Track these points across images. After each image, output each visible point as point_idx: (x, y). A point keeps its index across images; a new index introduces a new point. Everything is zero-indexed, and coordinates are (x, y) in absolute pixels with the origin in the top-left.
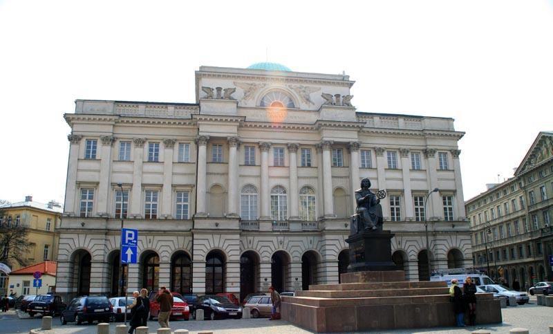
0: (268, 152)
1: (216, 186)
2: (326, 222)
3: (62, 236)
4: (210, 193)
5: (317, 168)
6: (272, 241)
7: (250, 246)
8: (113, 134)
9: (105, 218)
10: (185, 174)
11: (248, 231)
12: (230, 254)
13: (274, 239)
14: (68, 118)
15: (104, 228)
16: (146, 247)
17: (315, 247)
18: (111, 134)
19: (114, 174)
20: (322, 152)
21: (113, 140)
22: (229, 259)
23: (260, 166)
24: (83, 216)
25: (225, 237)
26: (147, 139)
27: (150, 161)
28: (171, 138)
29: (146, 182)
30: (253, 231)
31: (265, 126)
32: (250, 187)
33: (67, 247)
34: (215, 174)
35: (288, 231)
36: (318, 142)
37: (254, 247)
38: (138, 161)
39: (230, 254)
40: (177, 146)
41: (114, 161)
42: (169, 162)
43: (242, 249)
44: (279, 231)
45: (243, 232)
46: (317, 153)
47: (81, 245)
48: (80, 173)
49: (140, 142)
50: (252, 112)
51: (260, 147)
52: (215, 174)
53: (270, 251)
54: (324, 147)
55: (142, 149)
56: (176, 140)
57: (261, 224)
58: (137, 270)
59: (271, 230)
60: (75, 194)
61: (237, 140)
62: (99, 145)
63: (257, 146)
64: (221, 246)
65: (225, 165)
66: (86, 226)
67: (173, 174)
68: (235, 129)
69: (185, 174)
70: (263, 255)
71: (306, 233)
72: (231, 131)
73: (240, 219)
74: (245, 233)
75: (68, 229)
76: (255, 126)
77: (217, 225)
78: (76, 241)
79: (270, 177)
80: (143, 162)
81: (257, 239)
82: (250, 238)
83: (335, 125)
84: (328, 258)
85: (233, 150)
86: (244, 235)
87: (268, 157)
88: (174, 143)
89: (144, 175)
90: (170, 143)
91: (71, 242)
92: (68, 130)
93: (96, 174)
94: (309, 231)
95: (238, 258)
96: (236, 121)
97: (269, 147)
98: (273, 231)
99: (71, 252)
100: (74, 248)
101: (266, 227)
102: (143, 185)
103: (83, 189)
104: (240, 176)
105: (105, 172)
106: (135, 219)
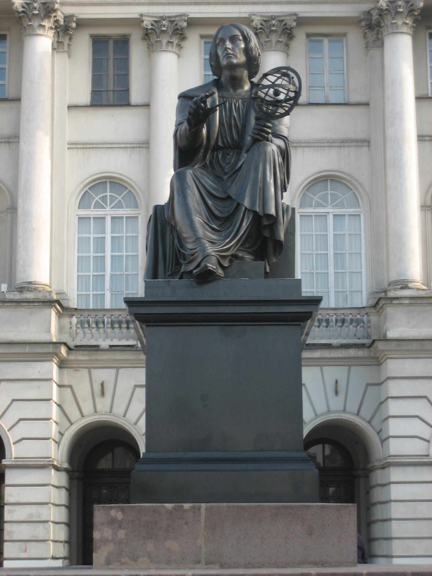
2: (389, 310)
5: (367, 104)
7: (103, 404)
11: (96, 348)
17: (352, 407)
20: (382, 46)
36: (366, 7)
37: (119, 409)
43: (74, 413)
46: (367, 47)
51: (147, 35)
54: (388, 20)
65: (13, 105)
84: (396, 447)
94: (329, 346)
95: (58, 453)
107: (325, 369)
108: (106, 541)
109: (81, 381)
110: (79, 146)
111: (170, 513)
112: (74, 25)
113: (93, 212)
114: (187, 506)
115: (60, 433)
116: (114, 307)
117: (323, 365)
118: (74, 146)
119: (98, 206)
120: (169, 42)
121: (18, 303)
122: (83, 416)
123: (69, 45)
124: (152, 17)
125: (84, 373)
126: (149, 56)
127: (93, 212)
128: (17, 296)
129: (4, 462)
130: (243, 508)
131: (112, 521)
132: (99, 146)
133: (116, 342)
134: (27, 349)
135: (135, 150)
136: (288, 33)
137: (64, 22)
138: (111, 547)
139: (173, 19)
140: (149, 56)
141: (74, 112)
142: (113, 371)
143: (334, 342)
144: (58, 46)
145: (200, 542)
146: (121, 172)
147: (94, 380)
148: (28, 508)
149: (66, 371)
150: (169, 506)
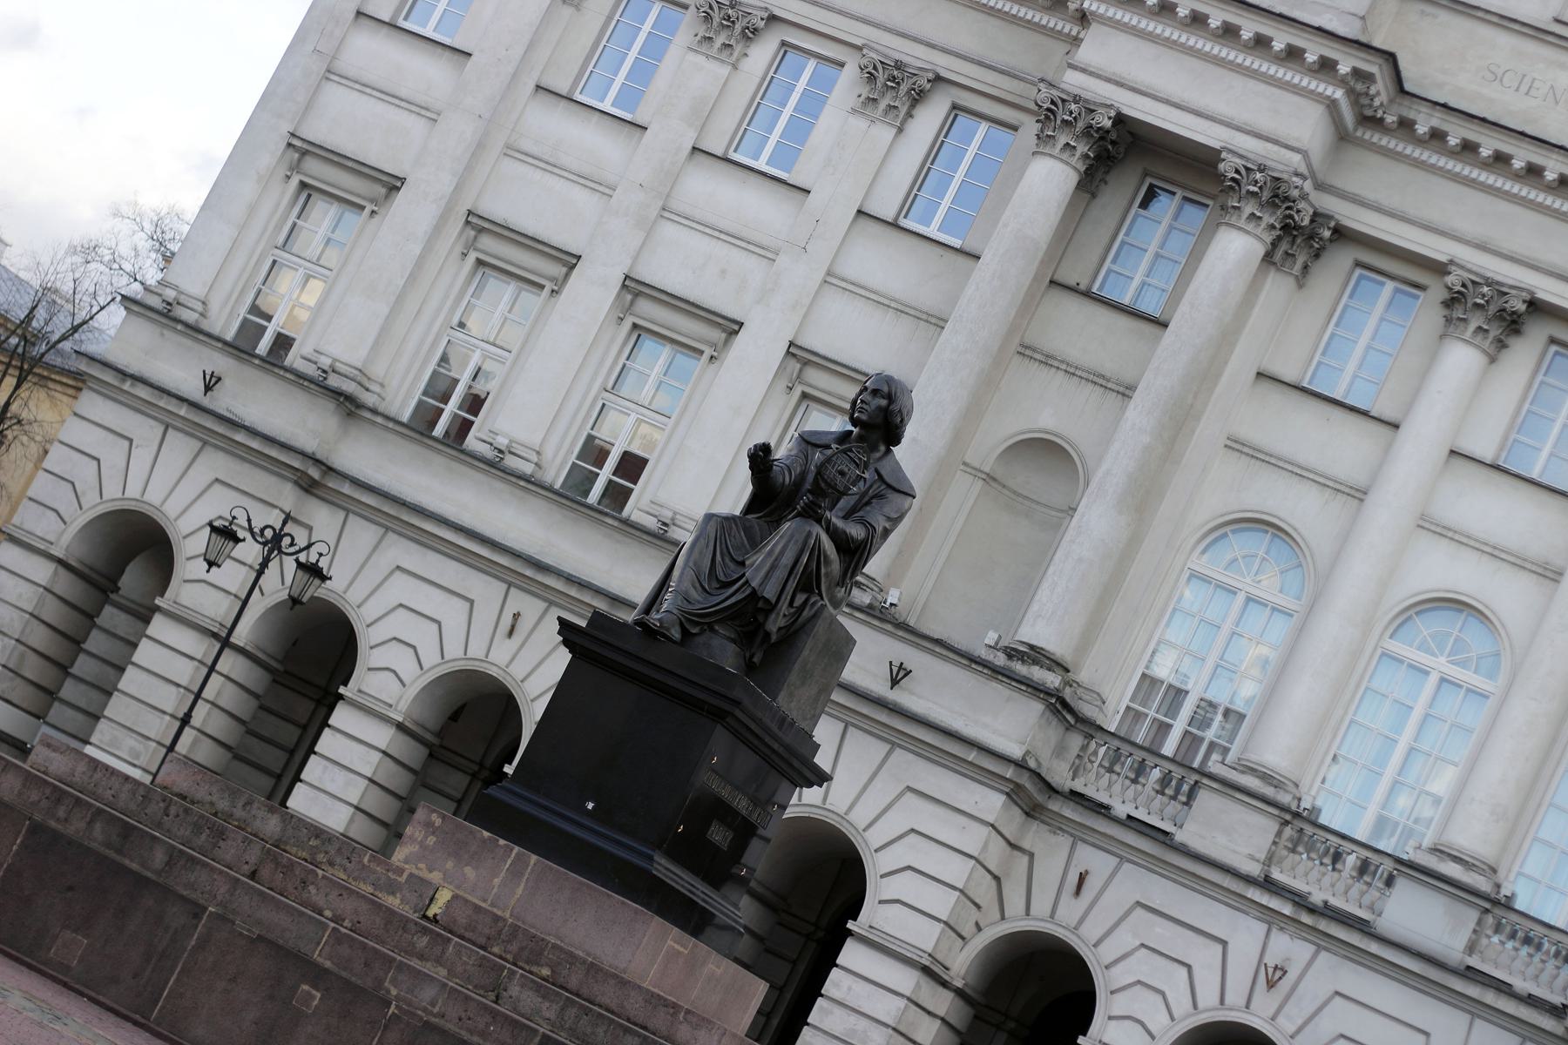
0: (1493, 360)
1: (1045, 450)
3: (92, 404)
4: (990, 478)
6: (1224, 943)
7: (1070, 910)
9: (337, 394)
10: (901, 309)
11: (1101, 809)
12: (891, 888)
13: (1245, 934)
15: (310, 445)
16: (476, 650)
19: (511, 167)
22: (871, 916)
24: (241, 348)
25: (401, 552)
28: (915, 56)
29: (658, 272)
31: (1501, 160)
33: (84, 472)
34: (1072, 371)
35: (1362, 926)
37: (1091, 931)
38: (670, 134)
39: (891, 888)
40: (930, 117)
41: (538, 87)
42: (834, 198)
43: (1015, 903)
44: (1299, 900)
45: (1033, 793)
47: (154, 496)
48: (337, 98)
50: (1505, 41)
51: (1454, 300)
52: (1072, 371)
53: (1181, 1004)
55: (725, 70)
56: (938, 79)
57: (1207, 800)
58: (368, 763)
59: (1254, 869)
60: (252, 209)
61: (1277, 195)
63: (1437, 293)
64: (860, 817)
66: (225, 400)
67: (831, 278)
69: (901, 309)
70: (1120, 1004)
71: (1473, 991)
72: (1266, 124)
73: (1061, 707)
74: (1069, 811)
75: (124, 374)
76: (1469, 148)
77: (898, 675)
78: (142, 458)
79: (1429, 525)
80: (695, 149)
81: (1136, 884)
83: (1469, 148)
85: (1237, 246)
86: (1058, 825)
87: (1479, 386)
88: (918, 97)
89: (669, 230)
91: (112, 454)
93: (415, 126)
94: (1503, 988)
96: (1326, 66)
97: (1512, 324)
98: (1268, 884)
99: (94, 506)
100: (112, 490)
101: (1229, 832)
102: (634, 288)
104: (1237, 446)
105: (459, 131)
106: (494, 465)
107: (1478, 1023)
108: (412, 840)
109: (1052, 853)
110: (1246, 450)
111: (484, 841)
112: (1327, 234)
114: (502, 842)
115: (977, 924)
116: (1178, 759)
117: (1479, 1017)
118: (1237, 446)
120: (1480, 328)
121: (996, 672)
122: (1028, 914)
123: (1306, 267)
124: (1470, 271)
125: (1064, 842)
126: (1442, 337)
128: (1000, 660)
129: (850, 925)
130: (551, 869)
131: (429, 824)
132: (1281, 464)
133: (1141, 814)
134: (972, 756)
135: (1340, 495)
137: (1312, 221)
138: (415, 848)
139: (1505, 289)
140: (1442, 337)
141: (1266, 386)
142: (1114, 861)
143: (1521, 985)
144: (1284, 260)
145: (497, 881)
146: (1297, 526)
147: (1074, 862)
148: (853, 1019)
149: (1035, 826)
150: (486, 834)
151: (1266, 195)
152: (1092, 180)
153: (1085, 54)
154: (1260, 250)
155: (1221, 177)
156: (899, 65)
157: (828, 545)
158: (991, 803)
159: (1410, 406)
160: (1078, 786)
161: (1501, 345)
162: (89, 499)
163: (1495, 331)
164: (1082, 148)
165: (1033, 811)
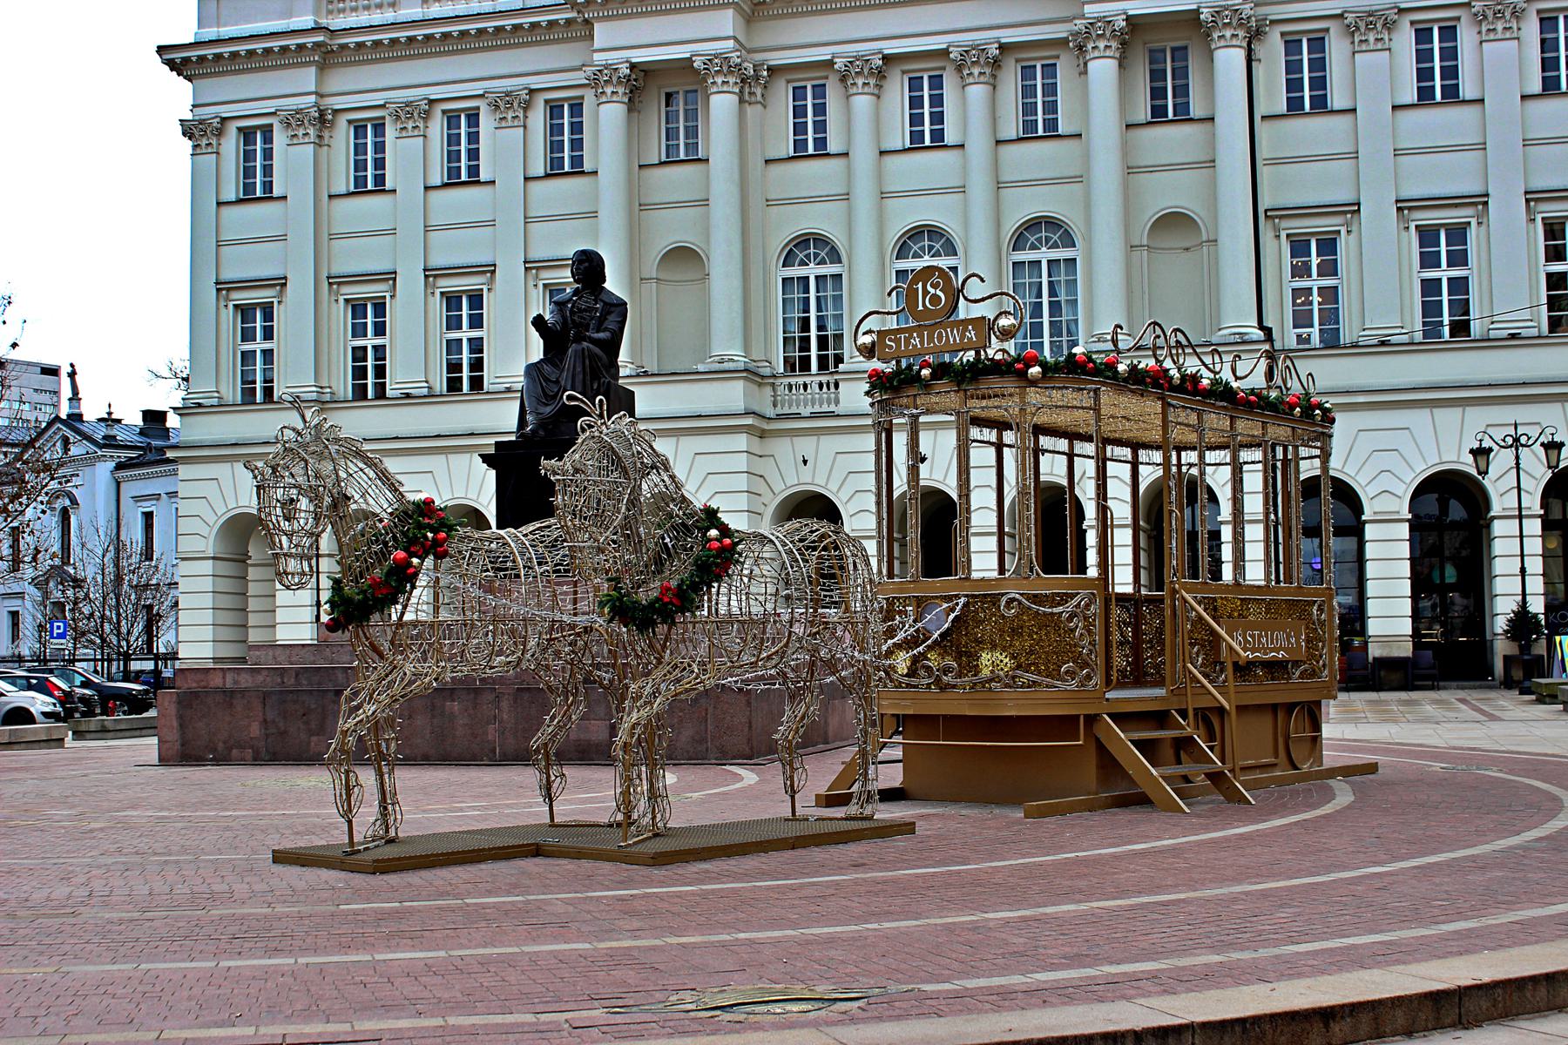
8: (322, 96)
11: (797, 417)
14: (178, 60)
18: (312, 98)
21: (324, 120)
23: (846, 154)
26: (432, 102)
27: (452, 181)
30: (814, 416)
32: (808, 245)
49: (414, 114)
56: (532, 92)
61: (731, 68)
62: (279, 138)
68: (725, 22)
82: (806, 445)
85: (722, 104)
88: (527, 106)
90: (512, 105)
92: (177, 96)
103: (241, 309)
113: (796, 272)
119: (803, 263)
127: (796, 272)
133: (817, 409)
136: (996, 64)
151: (725, 69)
152: (633, 105)
153: (598, 42)
154: (735, 98)
155: (697, 72)
156: (508, 94)
157: (597, 350)
158: (741, 441)
159: (849, 141)
160: (779, 411)
161: (879, 87)
162: (211, 519)
163: (872, 81)
164: (621, 90)
165: (763, 435)
